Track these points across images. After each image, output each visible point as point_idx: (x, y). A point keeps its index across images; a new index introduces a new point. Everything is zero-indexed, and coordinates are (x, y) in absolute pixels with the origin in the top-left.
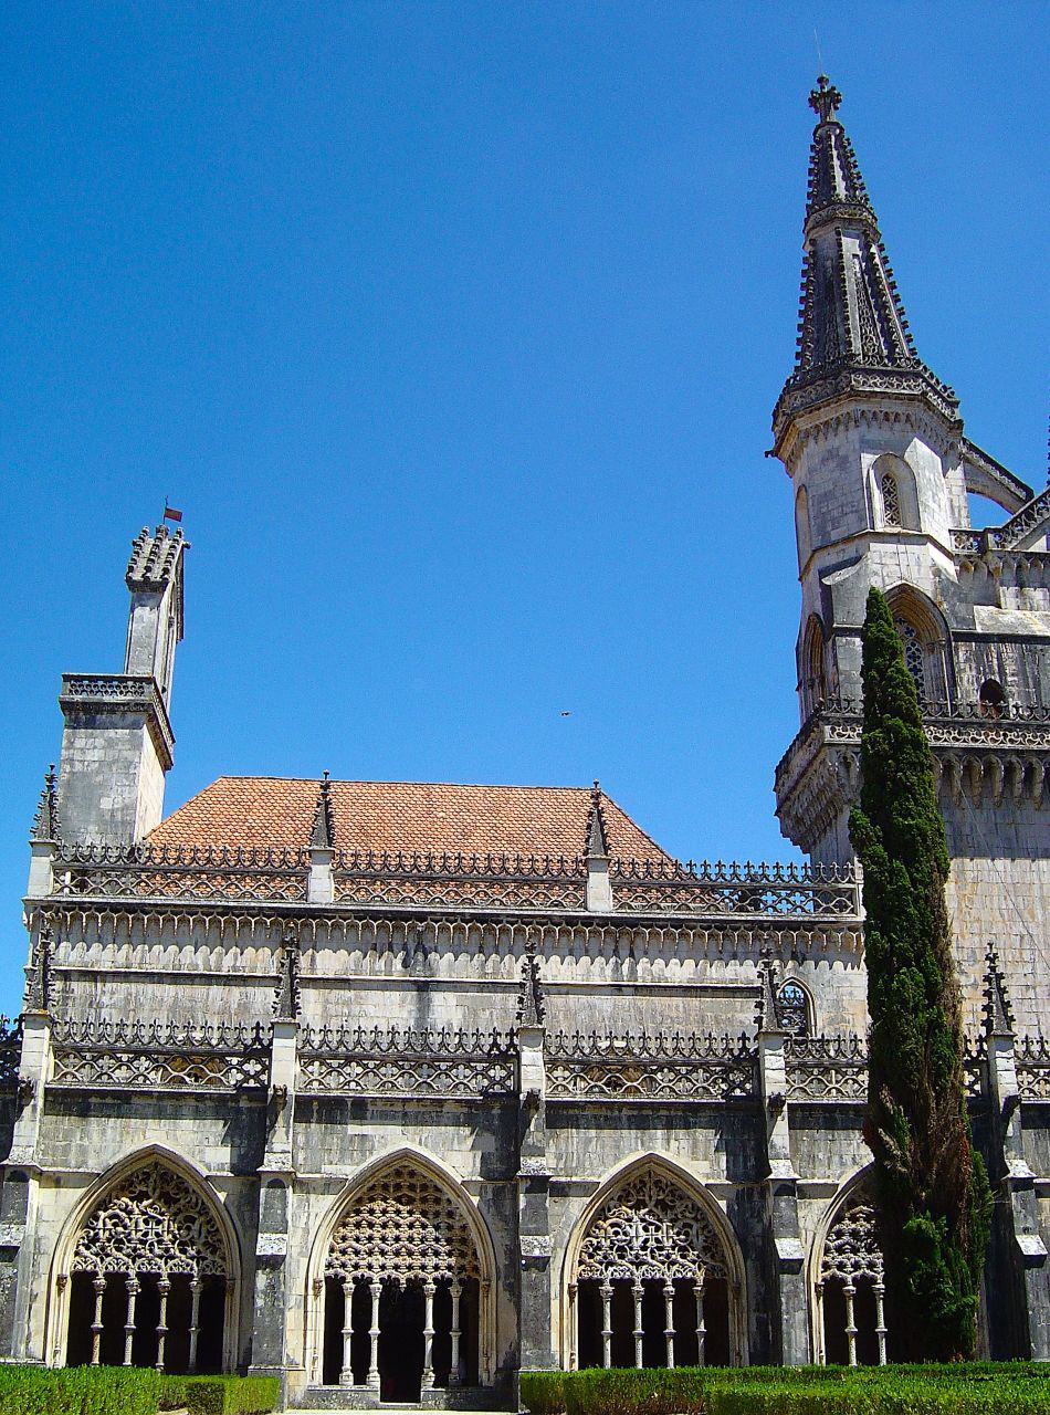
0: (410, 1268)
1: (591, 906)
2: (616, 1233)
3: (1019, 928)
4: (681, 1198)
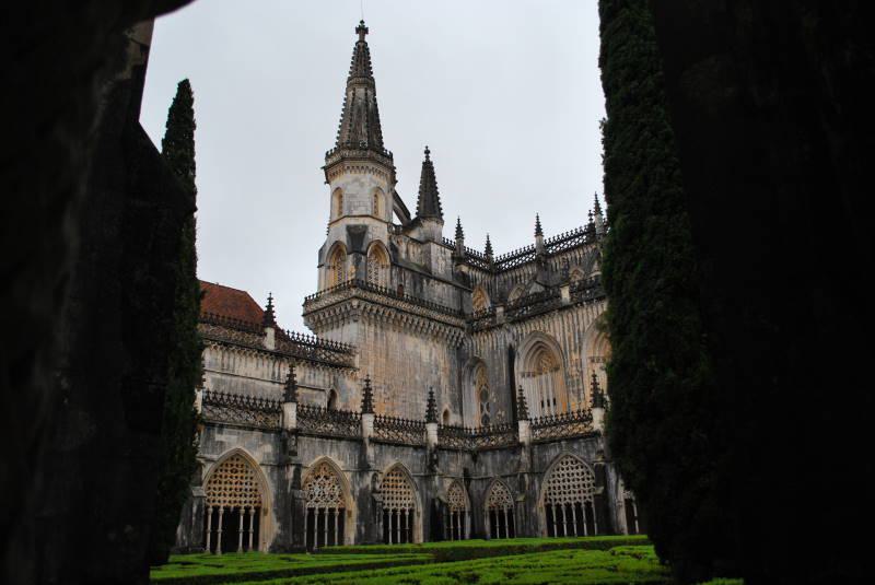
0: (235, 502)
3: (403, 379)
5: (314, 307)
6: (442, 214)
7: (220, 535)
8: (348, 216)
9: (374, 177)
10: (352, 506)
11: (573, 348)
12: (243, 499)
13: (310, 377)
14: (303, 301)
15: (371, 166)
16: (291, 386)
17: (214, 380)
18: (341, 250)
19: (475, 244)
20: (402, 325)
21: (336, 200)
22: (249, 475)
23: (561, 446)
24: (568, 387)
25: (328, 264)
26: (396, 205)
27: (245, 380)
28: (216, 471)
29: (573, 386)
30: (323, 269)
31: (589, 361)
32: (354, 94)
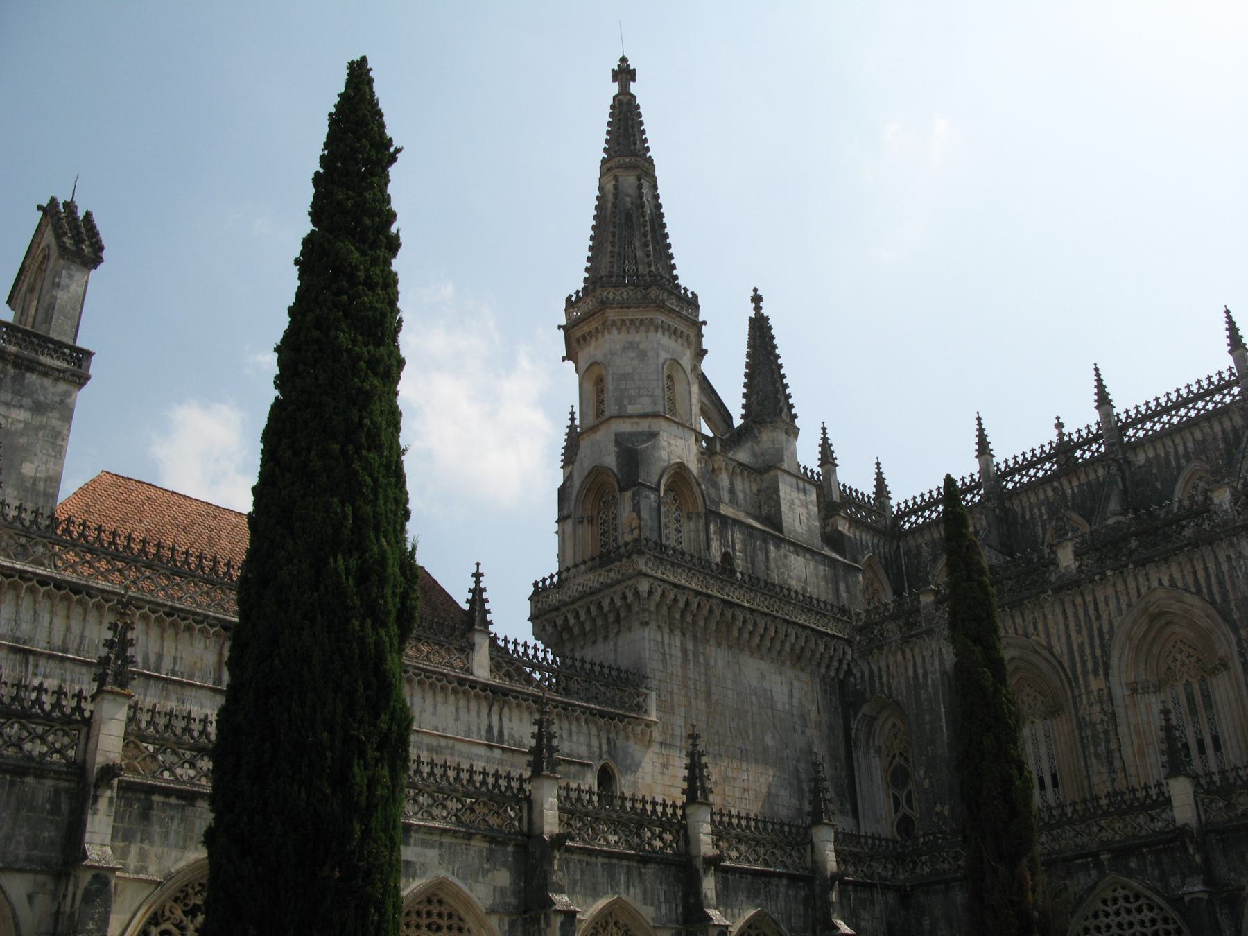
1: (475, 672)
5: (555, 598)
6: (795, 416)
8: (619, 417)
9: (665, 340)
11: (1090, 666)
14: (531, 590)
19: (855, 476)
20: (735, 633)
21: (589, 386)
23: (1098, 865)
24: (1084, 748)
25: (579, 513)
29: (1096, 745)
30: (569, 525)
31: (1127, 692)
32: (616, 187)
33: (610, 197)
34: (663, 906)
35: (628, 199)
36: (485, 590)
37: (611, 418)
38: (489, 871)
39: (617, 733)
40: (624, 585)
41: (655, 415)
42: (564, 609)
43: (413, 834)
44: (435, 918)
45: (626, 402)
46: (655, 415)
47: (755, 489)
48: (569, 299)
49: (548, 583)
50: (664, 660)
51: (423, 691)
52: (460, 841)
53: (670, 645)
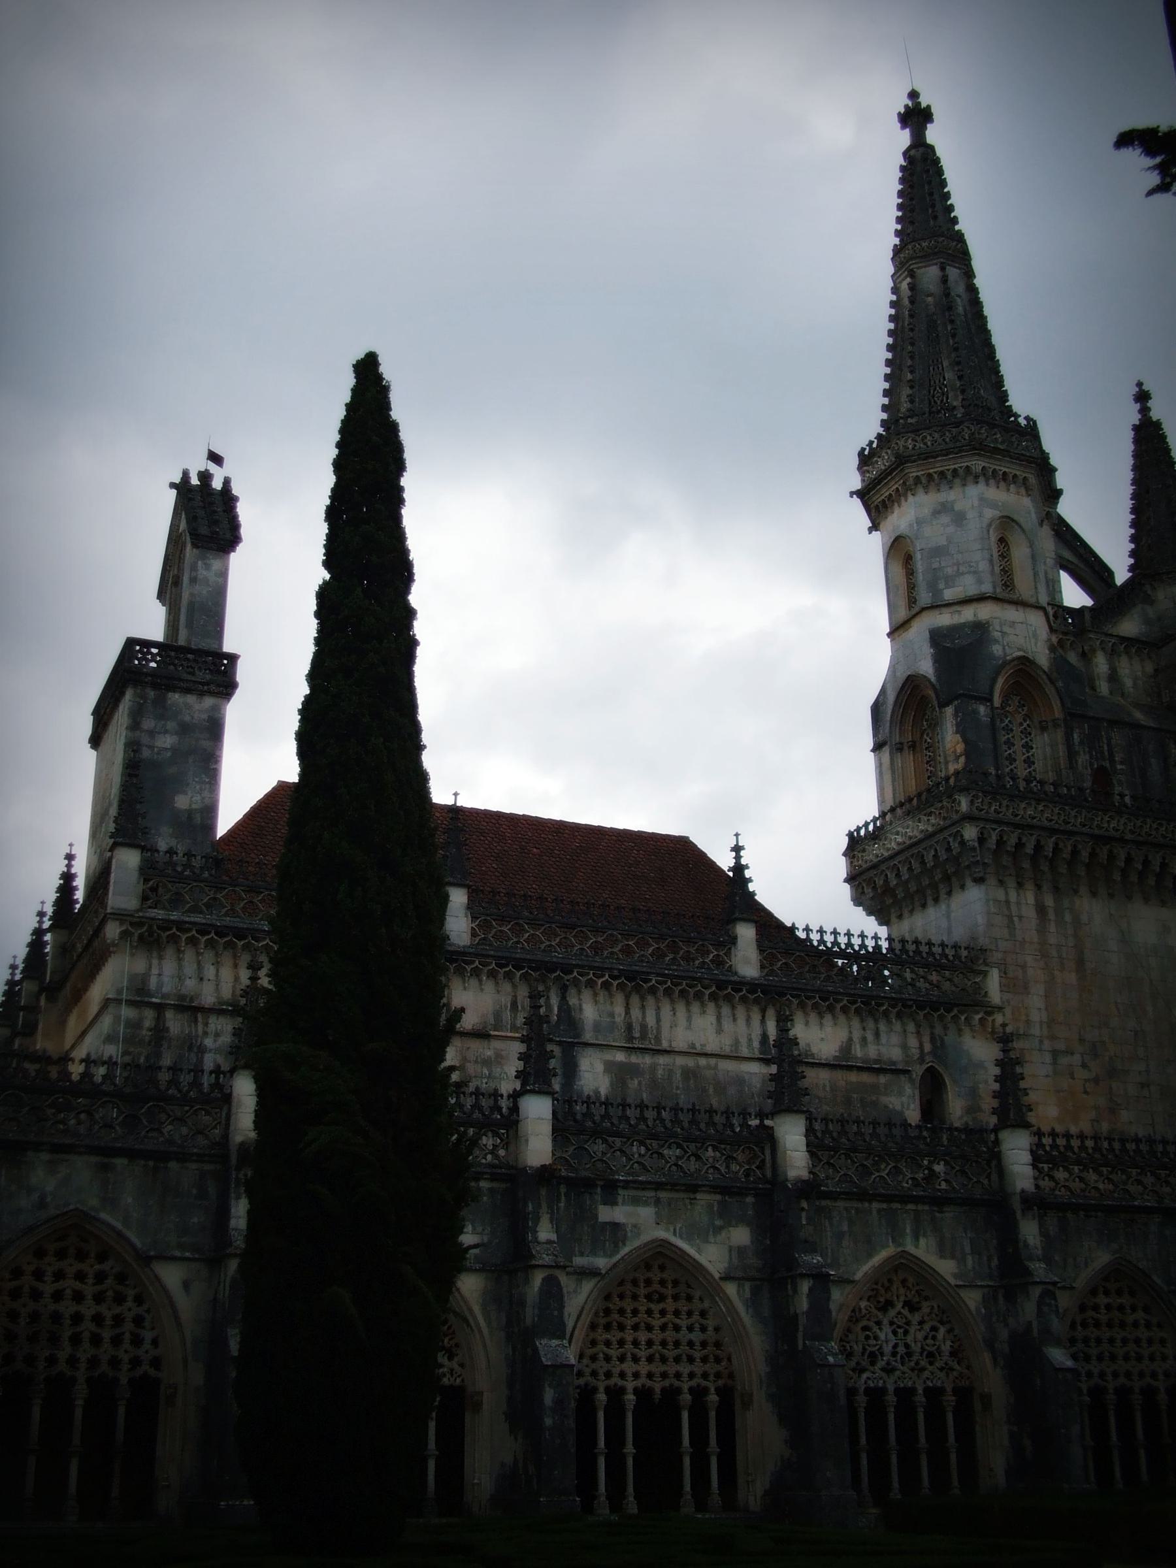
0: (664, 1375)
2: (867, 1338)
4: (926, 1299)
7: (630, 1462)
10: (992, 1380)
12: (685, 1369)
13: (864, 1040)
14: (844, 842)
15: (977, 464)
16: (785, 1057)
17: (610, 1067)
18: (924, 700)
21: (898, 570)
22: (697, 1305)
26: (1067, 554)
27: (690, 1062)
28: (608, 1297)
32: (912, 287)
33: (906, 302)
34: (969, 1258)
35: (930, 299)
36: (747, 867)
37: (923, 609)
38: (721, 1228)
39: (945, 1028)
40: (946, 834)
41: (980, 599)
42: (883, 867)
43: (620, 1192)
44: (656, 1286)
45: (941, 586)
46: (980, 599)
47: (1150, 668)
48: (861, 454)
49: (862, 832)
50: (1010, 925)
51: (672, 1002)
52: (682, 1195)
53: (1018, 903)
